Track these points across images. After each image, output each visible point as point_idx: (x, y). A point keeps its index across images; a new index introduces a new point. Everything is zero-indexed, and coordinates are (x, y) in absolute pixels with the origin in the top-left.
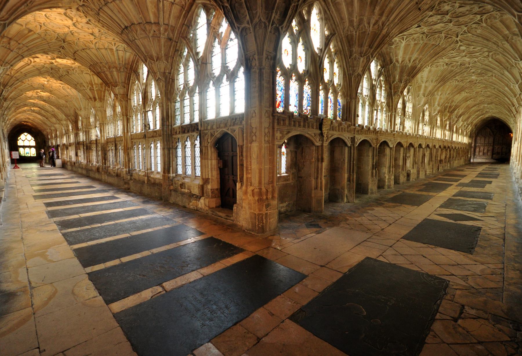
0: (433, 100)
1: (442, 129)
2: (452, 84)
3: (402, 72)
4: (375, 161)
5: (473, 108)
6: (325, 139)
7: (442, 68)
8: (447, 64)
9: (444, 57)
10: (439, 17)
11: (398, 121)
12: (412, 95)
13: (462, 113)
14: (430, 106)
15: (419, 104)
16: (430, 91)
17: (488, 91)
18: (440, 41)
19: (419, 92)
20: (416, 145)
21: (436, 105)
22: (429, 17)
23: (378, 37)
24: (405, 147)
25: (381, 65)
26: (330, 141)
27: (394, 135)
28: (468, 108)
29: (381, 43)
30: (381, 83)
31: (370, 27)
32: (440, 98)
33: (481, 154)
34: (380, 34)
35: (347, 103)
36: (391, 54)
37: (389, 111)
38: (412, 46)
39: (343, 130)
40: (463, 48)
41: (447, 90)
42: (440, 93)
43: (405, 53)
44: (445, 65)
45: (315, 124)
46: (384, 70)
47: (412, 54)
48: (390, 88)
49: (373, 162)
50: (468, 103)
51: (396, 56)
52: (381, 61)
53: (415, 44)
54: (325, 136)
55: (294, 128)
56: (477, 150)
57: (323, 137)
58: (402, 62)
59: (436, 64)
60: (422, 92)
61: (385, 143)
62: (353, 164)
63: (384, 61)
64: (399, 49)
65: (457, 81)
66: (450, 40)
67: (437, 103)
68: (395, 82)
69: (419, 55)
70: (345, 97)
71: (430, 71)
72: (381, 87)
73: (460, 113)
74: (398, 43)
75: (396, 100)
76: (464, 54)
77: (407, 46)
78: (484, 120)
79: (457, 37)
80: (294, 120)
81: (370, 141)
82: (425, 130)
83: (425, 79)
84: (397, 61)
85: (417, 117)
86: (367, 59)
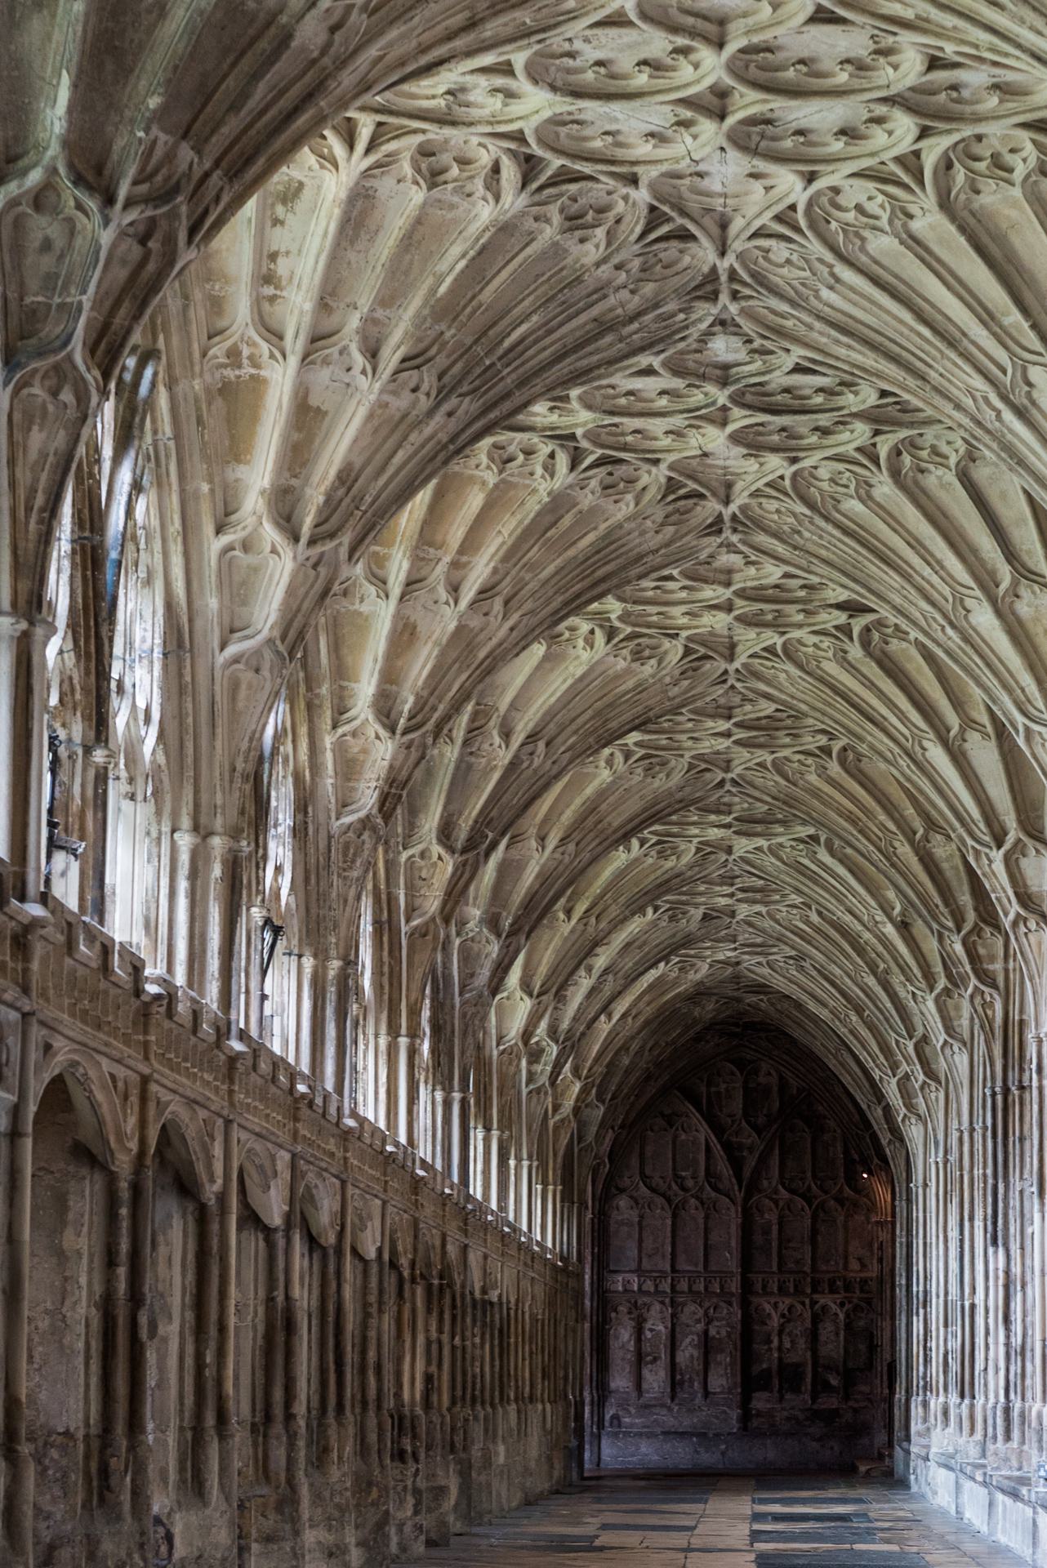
0: (336, 647)
1: (393, 1031)
5: (620, 858)
7: (485, 213)
8: (529, 166)
12: (160, 483)
13: (545, 879)
15: (231, 631)
16: (346, 478)
17: (789, 653)
19: (241, 471)
24: (123, 1164)
32: (404, 636)
33: (656, 1379)
41: (470, 544)
42: (398, 568)
44: (510, 173)
50: (601, 775)
56: (623, 1336)
59: (435, 133)
65: (562, 460)
67: (365, 688)
68: (35, 177)
73: (529, 877)
75: (36, 438)
78: (665, 1018)
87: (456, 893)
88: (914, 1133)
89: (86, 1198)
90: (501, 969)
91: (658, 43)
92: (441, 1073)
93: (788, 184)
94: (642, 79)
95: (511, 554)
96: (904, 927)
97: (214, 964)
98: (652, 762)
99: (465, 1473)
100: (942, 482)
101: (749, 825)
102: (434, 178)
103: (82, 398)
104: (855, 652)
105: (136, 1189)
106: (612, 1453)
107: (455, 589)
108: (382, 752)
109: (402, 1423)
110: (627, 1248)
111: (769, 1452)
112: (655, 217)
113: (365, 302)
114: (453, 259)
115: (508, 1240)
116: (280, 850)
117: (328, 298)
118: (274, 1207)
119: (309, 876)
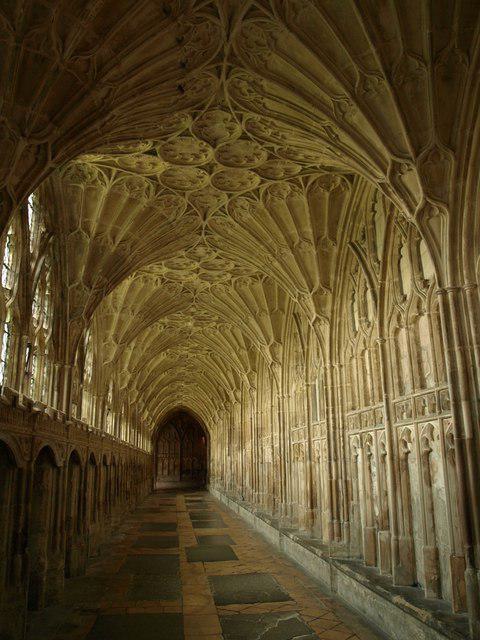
8: (163, 280)
9: (163, 263)
10: (196, 145)
13: (153, 393)
15: (105, 360)
20: (99, 460)
21: (125, 369)
22: (181, 135)
24: (83, 464)
25: (46, 226)
28: (162, 385)
29: (84, 128)
32: (133, 356)
33: (166, 472)
36: (75, 205)
37: (57, 360)
38: (124, 201)
40: (201, 251)
44: (159, 281)
46: (54, 241)
47: (121, 221)
48: (63, 296)
51: (87, 214)
52: (48, 215)
56: (160, 464)
58: (97, 234)
60: (112, 332)
61: (47, 454)
64: (96, 199)
69: (133, 230)
71: (132, 287)
74: (94, 182)
77: (113, 197)
79: (205, 219)
83: (120, 303)
84: (87, 229)
85: (99, 388)
86: (38, 153)
87: (138, 398)
88: (211, 432)
89: (76, 471)
91: (188, 261)
93: (208, 284)
94: (184, 266)
95: (154, 343)
96: (212, 400)
97: (100, 420)
100: (228, 332)
103: (83, 324)
104: (209, 357)
105: (86, 468)
106: (158, 485)
107: (143, 349)
108: (129, 376)
110: (161, 450)
111: (184, 485)
113: (132, 303)
114: (148, 296)
115: (145, 454)
116: (110, 394)
117: (126, 300)
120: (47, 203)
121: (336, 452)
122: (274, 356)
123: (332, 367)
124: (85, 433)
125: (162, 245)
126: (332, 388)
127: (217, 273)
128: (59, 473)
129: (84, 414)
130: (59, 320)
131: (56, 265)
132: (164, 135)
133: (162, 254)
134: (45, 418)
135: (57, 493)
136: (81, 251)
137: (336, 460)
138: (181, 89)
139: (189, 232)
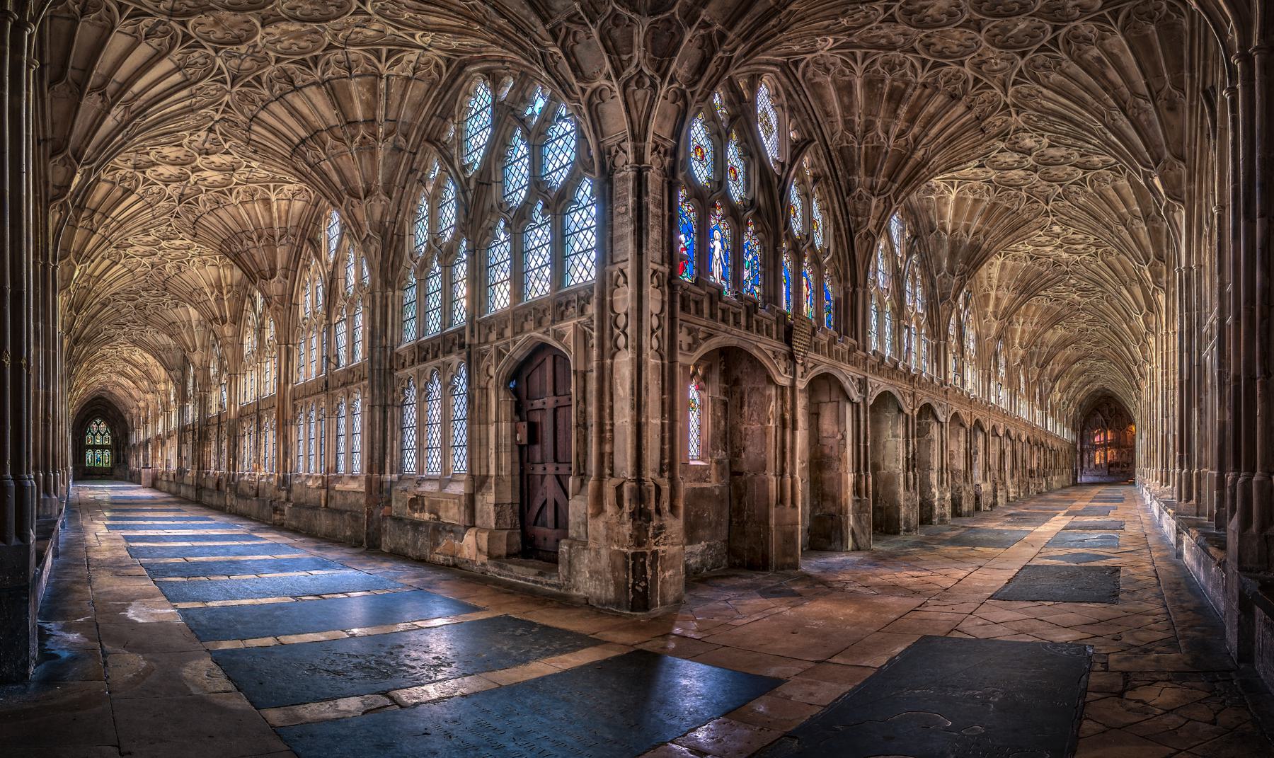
2: (1042, 302)
3: (953, 254)
4: (911, 449)
5: (1075, 366)
6: (800, 370)
8: (1031, 257)
11: (952, 364)
13: (1060, 371)
14: (1006, 344)
16: (1005, 309)
18: (1020, 205)
23: (906, 163)
24: (968, 426)
25: (911, 232)
26: (810, 377)
27: (946, 392)
28: (1069, 363)
29: (913, 177)
30: (913, 270)
31: (888, 139)
32: (1023, 332)
34: (910, 157)
35: (846, 294)
36: (931, 212)
39: (838, 356)
40: (1056, 229)
41: (1034, 315)
42: (1021, 320)
43: (956, 214)
45: (774, 327)
47: (970, 218)
48: (933, 285)
49: (908, 453)
50: (1068, 351)
51: (942, 217)
53: (976, 201)
54: (800, 362)
55: (723, 326)
57: (796, 362)
58: (953, 231)
60: (991, 309)
62: (866, 447)
63: (916, 224)
64: (946, 204)
66: (1035, 206)
69: (983, 223)
70: (840, 281)
71: (1003, 266)
72: (914, 277)
73: (1056, 371)
74: (942, 192)
76: (1059, 241)
77: (960, 201)
79: (1047, 204)
80: (723, 305)
81: (899, 397)
82: (1000, 396)
83: (995, 282)
84: (944, 230)
85: (987, 361)
90: (1053, 388)
91: (1049, 238)
92: (1042, 406)
95: (1040, 317)
98: (1077, 349)
99: (1047, 481)
101: (1098, 360)
102: (1015, 260)
108: (1021, 352)
109: (1031, 471)
112: (1054, 263)
114: (1020, 273)
116: (1002, 370)
118: (1001, 433)
119: (1009, 374)
120: (911, 214)
121: (1167, 410)
122: (1147, 327)
123: (1167, 333)
124: (971, 401)
125: (1016, 229)
126: (1167, 353)
127: (1082, 246)
128: (942, 427)
129: (969, 386)
130: (932, 303)
131: (923, 260)
132: (986, 155)
133: (1018, 237)
134: (923, 381)
135: (942, 442)
136: (942, 247)
137: (1167, 417)
138: (983, 130)
139: (1036, 217)
